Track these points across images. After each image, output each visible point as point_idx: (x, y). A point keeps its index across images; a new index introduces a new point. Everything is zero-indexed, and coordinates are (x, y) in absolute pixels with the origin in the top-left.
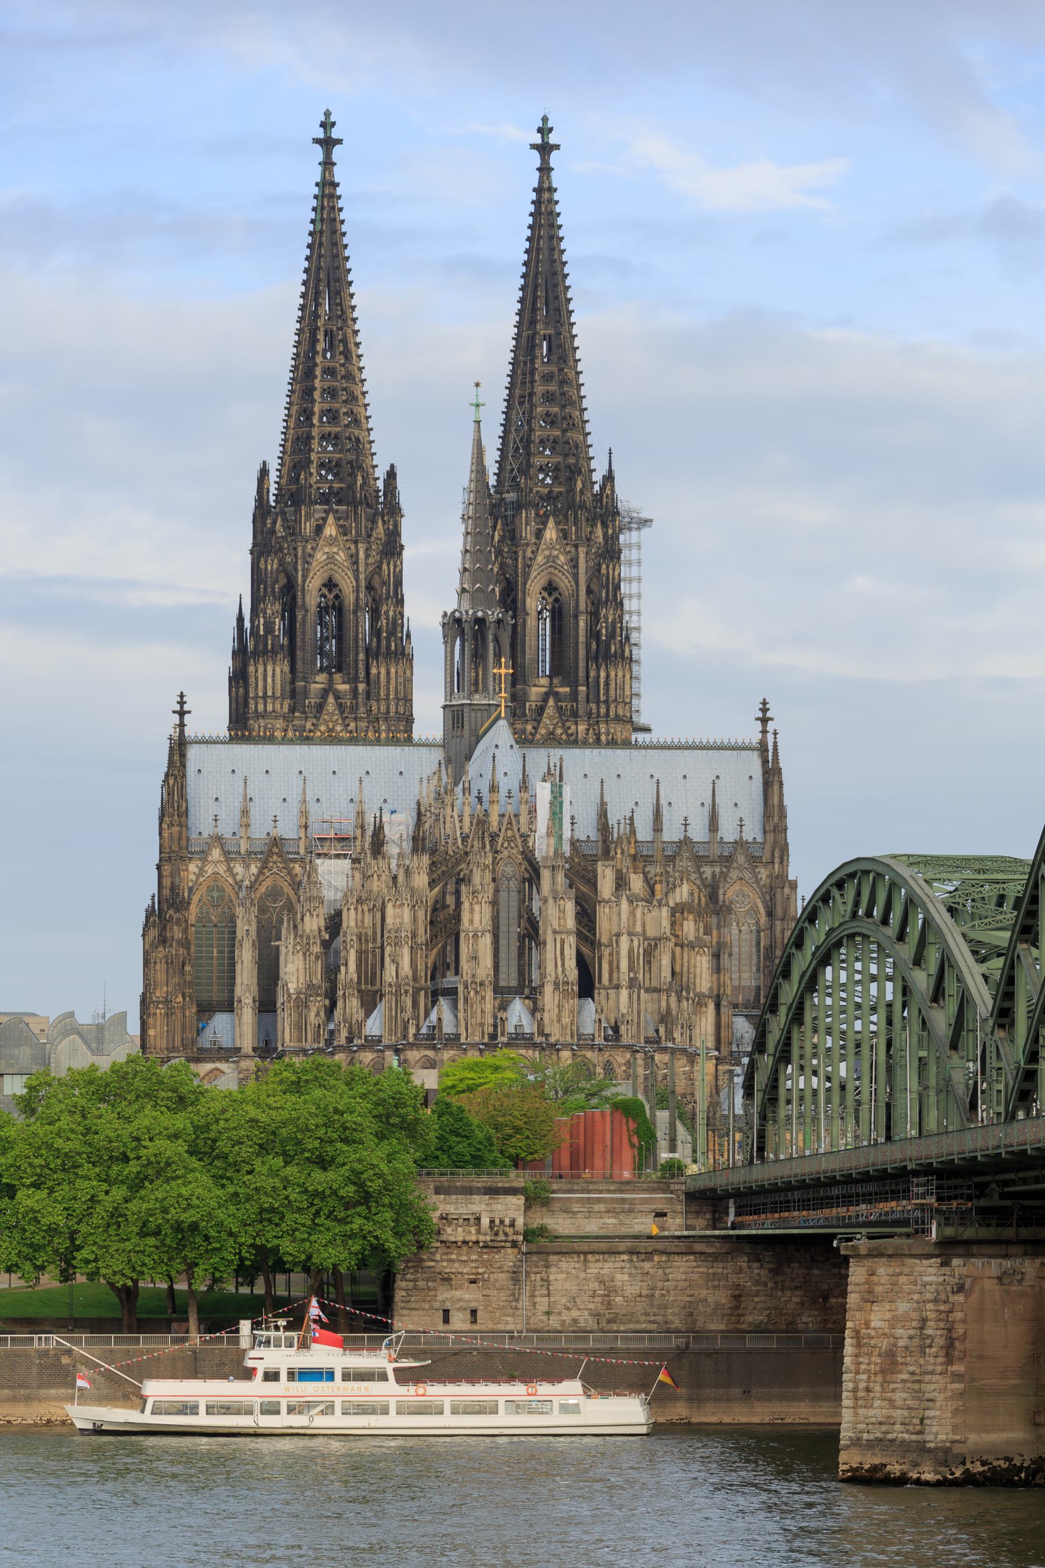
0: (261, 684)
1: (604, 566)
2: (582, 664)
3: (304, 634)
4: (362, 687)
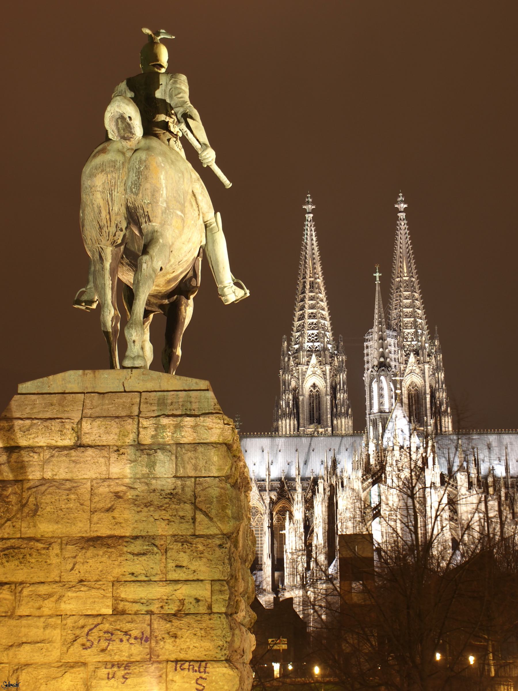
0: (284, 429)
1: (436, 374)
3: (303, 407)
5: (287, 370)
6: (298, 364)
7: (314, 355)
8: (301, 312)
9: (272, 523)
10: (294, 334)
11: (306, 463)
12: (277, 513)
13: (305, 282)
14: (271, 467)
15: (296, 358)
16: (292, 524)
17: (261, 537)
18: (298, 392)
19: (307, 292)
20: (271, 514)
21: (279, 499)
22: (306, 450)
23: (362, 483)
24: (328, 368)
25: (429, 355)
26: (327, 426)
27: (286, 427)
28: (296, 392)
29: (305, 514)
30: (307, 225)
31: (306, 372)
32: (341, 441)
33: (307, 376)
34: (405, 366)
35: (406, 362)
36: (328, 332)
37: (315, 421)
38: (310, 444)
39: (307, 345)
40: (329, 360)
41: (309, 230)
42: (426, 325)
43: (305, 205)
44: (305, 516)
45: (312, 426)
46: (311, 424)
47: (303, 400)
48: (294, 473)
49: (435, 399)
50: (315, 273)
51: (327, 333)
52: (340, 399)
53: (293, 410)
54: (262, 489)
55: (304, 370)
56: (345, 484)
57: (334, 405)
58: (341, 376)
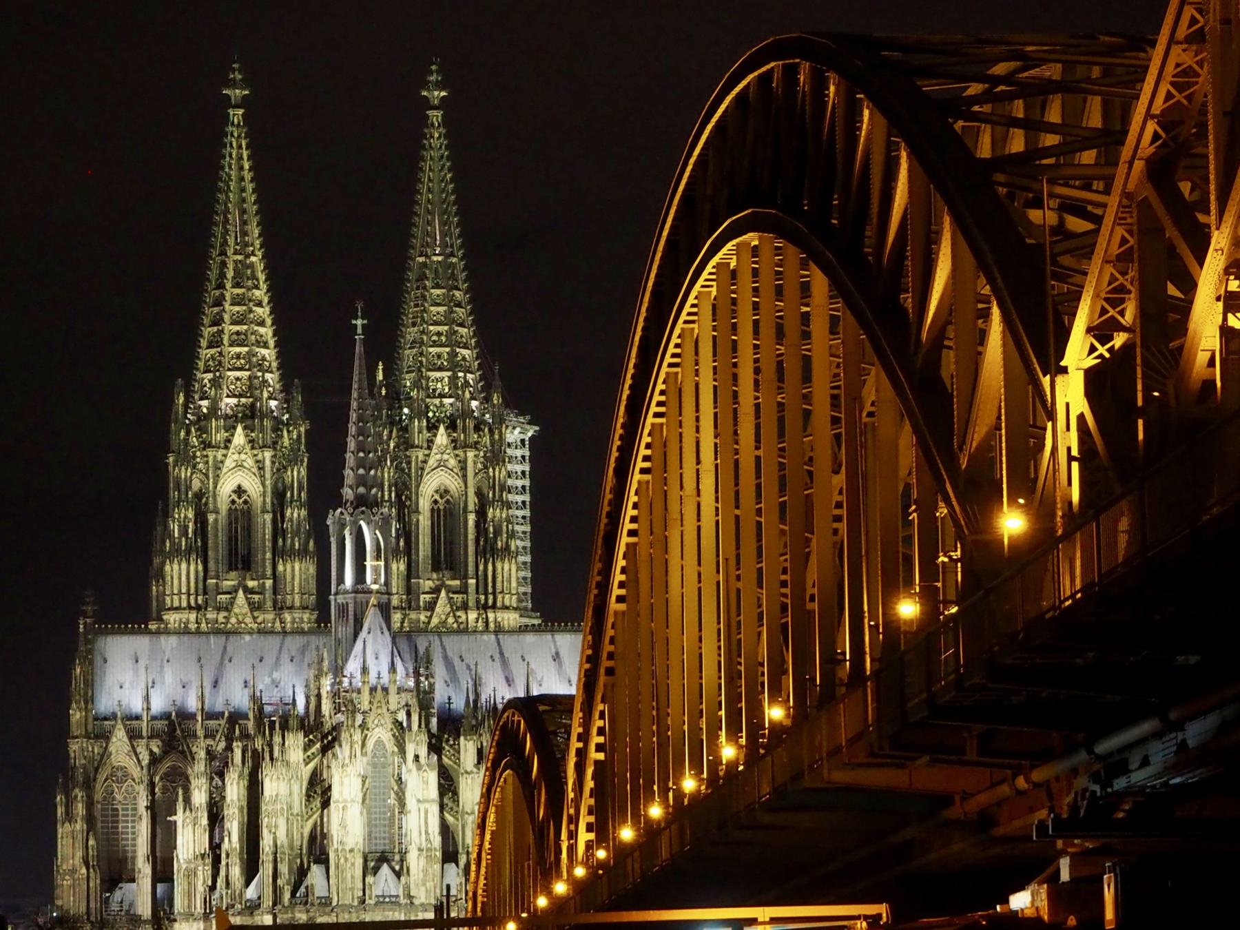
0: (176, 582)
2: (471, 559)
4: (269, 583)
5: (187, 459)
6: (207, 445)
7: (239, 429)
8: (215, 329)
9: (153, 801)
10: (199, 375)
11: (215, 684)
12: (161, 779)
13: (224, 264)
14: (152, 691)
16: (188, 812)
17: (133, 827)
18: (206, 504)
19: (228, 285)
20: (152, 785)
21: (166, 753)
22: (218, 658)
23: (305, 750)
24: (268, 454)
25: (477, 429)
26: (264, 577)
27: (180, 579)
28: (201, 503)
29: (211, 794)
30: (232, 135)
31: (222, 462)
32: (282, 644)
33: (225, 470)
34: (427, 452)
35: (430, 443)
36: (271, 372)
37: (240, 566)
38: (225, 648)
40: (270, 436)
41: (234, 144)
42: (477, 358)
43: (228, 87)
44: (211, 798)
45: (233, 574)
46: (231, 569)
47: (216, 520)
48: (193, 704)
49: (485, 521)
50: (247, 245)
51: (268, 376)
52: (291, 520)
53: (196, 541)
54: (134, 735)
55: (220, 457)
56: (276, 754)
57: (278, 531)
58: (295, 473)
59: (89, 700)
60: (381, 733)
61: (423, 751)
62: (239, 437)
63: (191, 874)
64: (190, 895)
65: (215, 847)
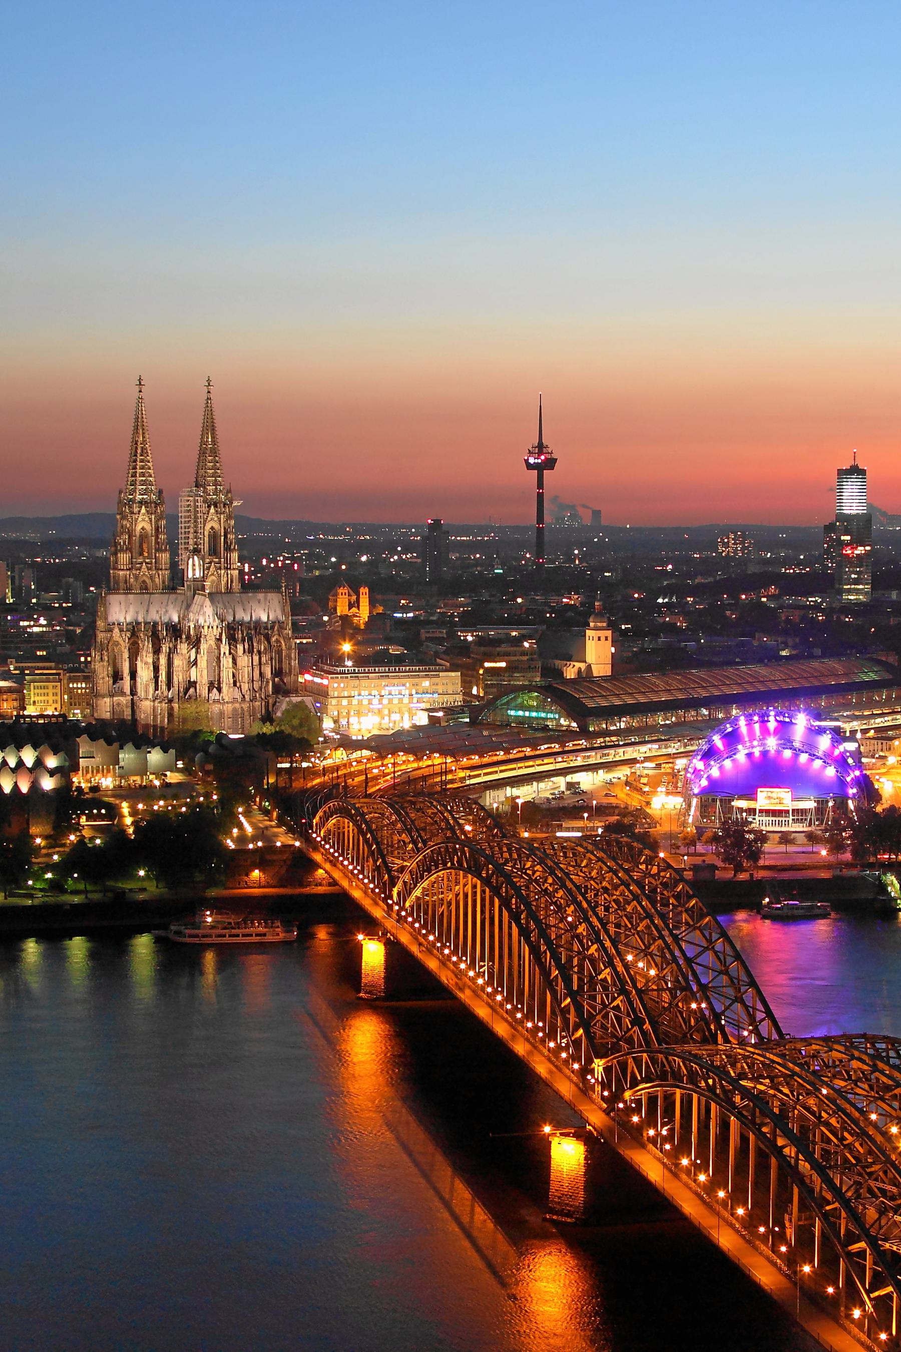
6: (133, 513)
13: (136, 448)
15: (130, 507)
35: (208, 512)
39: (139, 497)
48: (140, 619)
54: (121, 631)
57: (157, 543)
59: (106, 619)
60: (212, 642)
61: (227, 653)
62: (143, 510)
63: (147, 686)
64: (146, 692)
65: (156, 678)
